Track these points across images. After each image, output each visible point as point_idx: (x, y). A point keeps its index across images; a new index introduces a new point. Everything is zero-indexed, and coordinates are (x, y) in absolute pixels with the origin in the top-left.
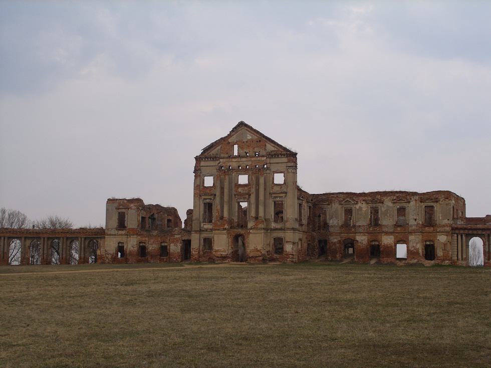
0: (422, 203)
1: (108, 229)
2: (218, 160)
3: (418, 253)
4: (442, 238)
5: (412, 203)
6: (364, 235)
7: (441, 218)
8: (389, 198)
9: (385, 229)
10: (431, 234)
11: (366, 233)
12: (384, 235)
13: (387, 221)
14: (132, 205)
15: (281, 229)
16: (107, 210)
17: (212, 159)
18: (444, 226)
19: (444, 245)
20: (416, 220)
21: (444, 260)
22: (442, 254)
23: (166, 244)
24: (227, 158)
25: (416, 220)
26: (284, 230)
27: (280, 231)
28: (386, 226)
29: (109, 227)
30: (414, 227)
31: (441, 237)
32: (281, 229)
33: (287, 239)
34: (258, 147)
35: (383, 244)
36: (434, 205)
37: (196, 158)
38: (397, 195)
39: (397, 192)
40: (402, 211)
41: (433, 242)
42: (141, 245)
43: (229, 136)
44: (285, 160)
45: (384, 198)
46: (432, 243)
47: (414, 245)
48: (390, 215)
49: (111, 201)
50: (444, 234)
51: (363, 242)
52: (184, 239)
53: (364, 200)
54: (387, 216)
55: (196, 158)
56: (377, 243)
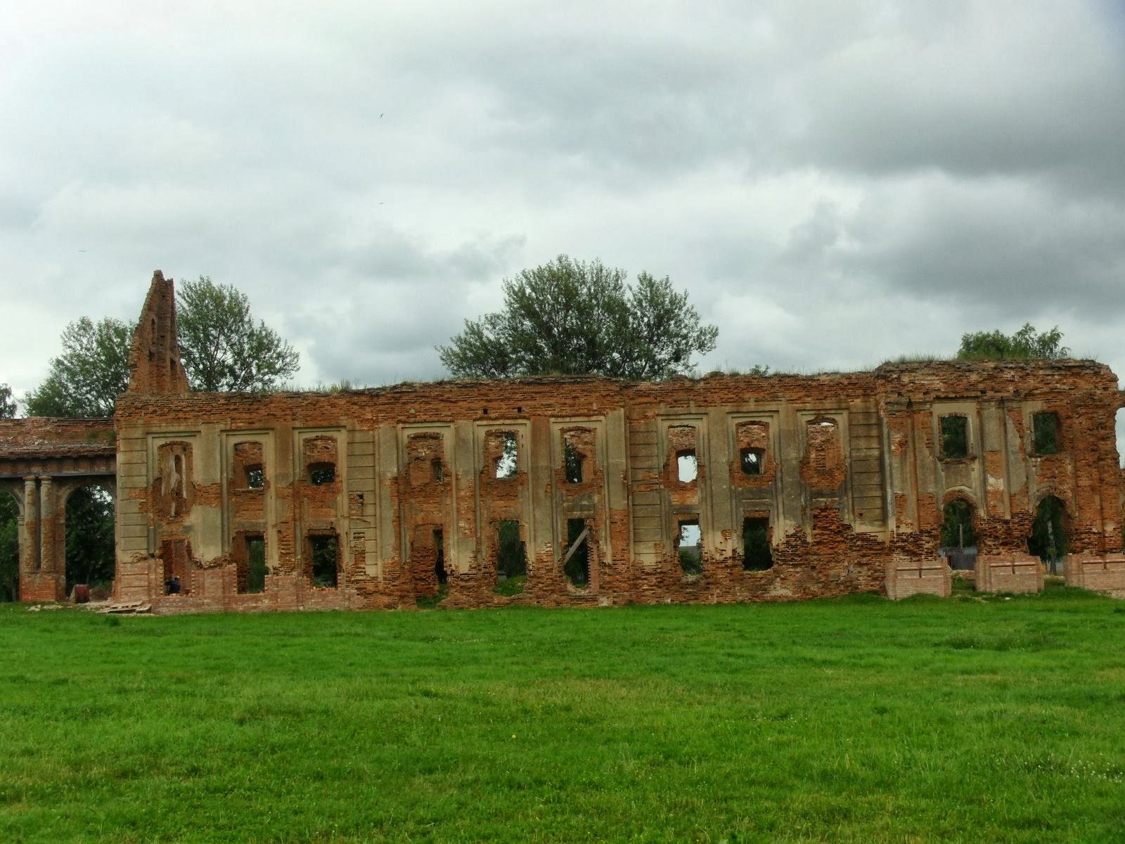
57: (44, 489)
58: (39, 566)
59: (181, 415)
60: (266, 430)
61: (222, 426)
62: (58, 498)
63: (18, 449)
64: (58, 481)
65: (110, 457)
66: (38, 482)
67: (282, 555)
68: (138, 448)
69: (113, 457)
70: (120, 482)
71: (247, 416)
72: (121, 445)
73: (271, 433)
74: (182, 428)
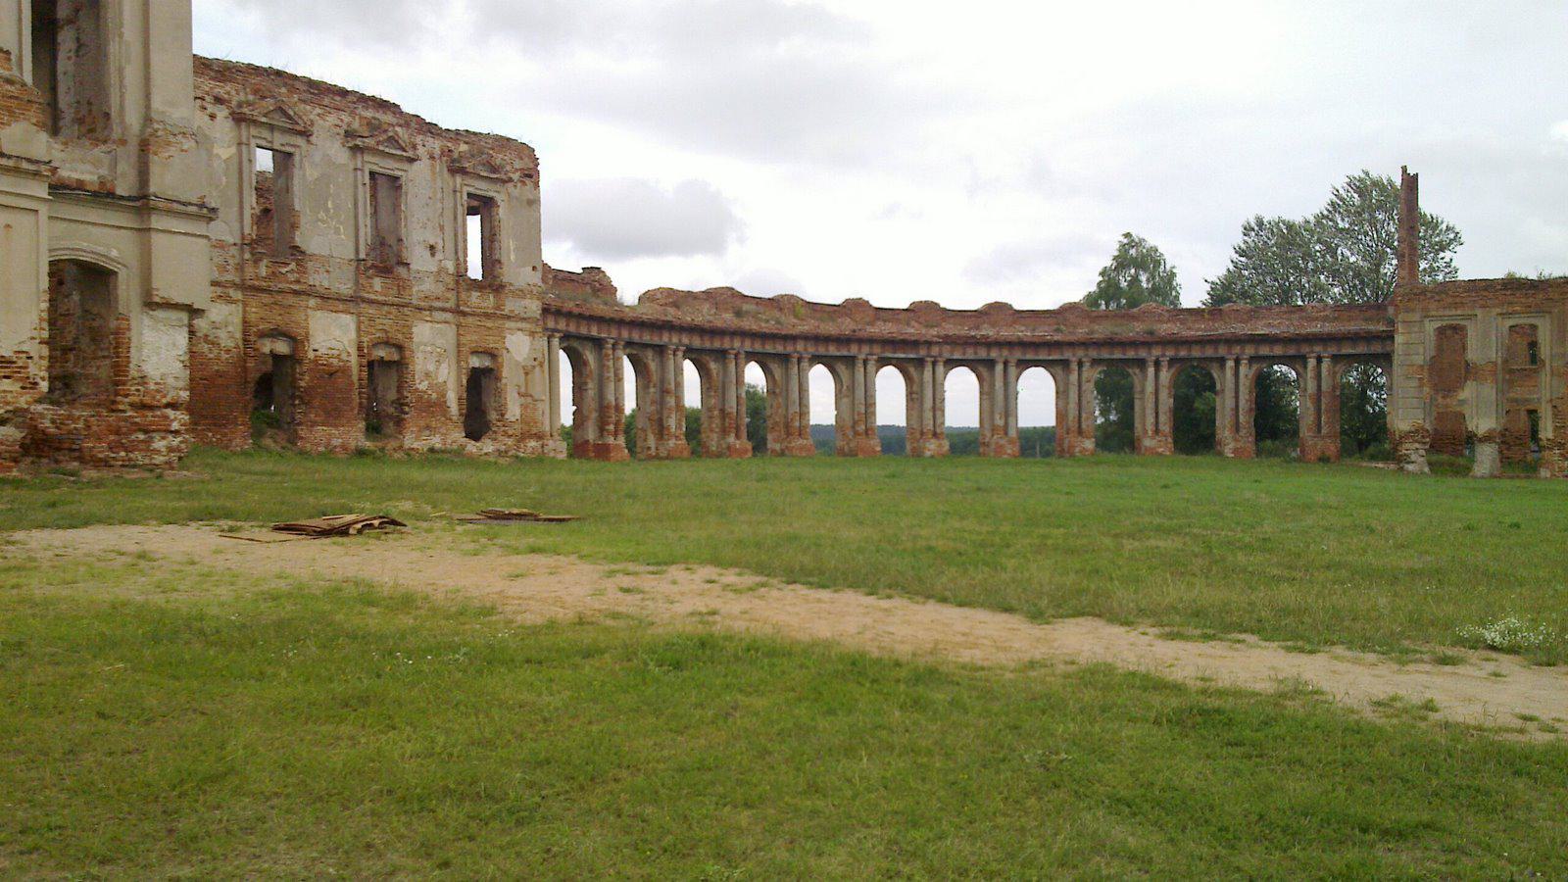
0: (459, 179)
3: (441, 405)
4: (519, 346)
5: (421, 168)
6: (230, 301)
7: (512, 257)
8: (332, 119)
9: (318, 279)
10: (489, 324)
11: (235, 285)
12: (318, 308)
13: (330, 236)
15: (103, 196)
18: (521, 294)
19: (527, 374)
20: (432, 248)
21: (523, 437)
22: (518, 412)
25: (432, 248)
26: (142, 203)
27: (94, 214)
28: (325, 261)
30: (428, 286)
31: (513, 338)
32: (103, 196)
33: (166, 286)
35: (311, 355)
36: (499, 198)
38: (369, 114)
39: (364, 99)
40: (386, 188)
41: (493, 355)
45: (310, 113)
46: (487, 363)
47: (431, 368)
48: (337, 207)
50: (524, 325)
51: (222, 334)
53: (218, 100)
54: (327, 210)
56: (282, 347)
57: (1325, 365)
58: (1319, 431)
59: (1458, 300)
60: (1540, 311)
61: (1498, 310)
62: (1335, 373)
63: (1303, 332)
64: (1336, 359)
65: (1390, 337)
66: (1319, 360)
67: (1556, 428)
68: (1416, 329)
69: (1392, 338)
70: (1397, 359)
71: (1523, 300)
72: (1400, 328)
73: (1547, 316)
74: (1459, 312)
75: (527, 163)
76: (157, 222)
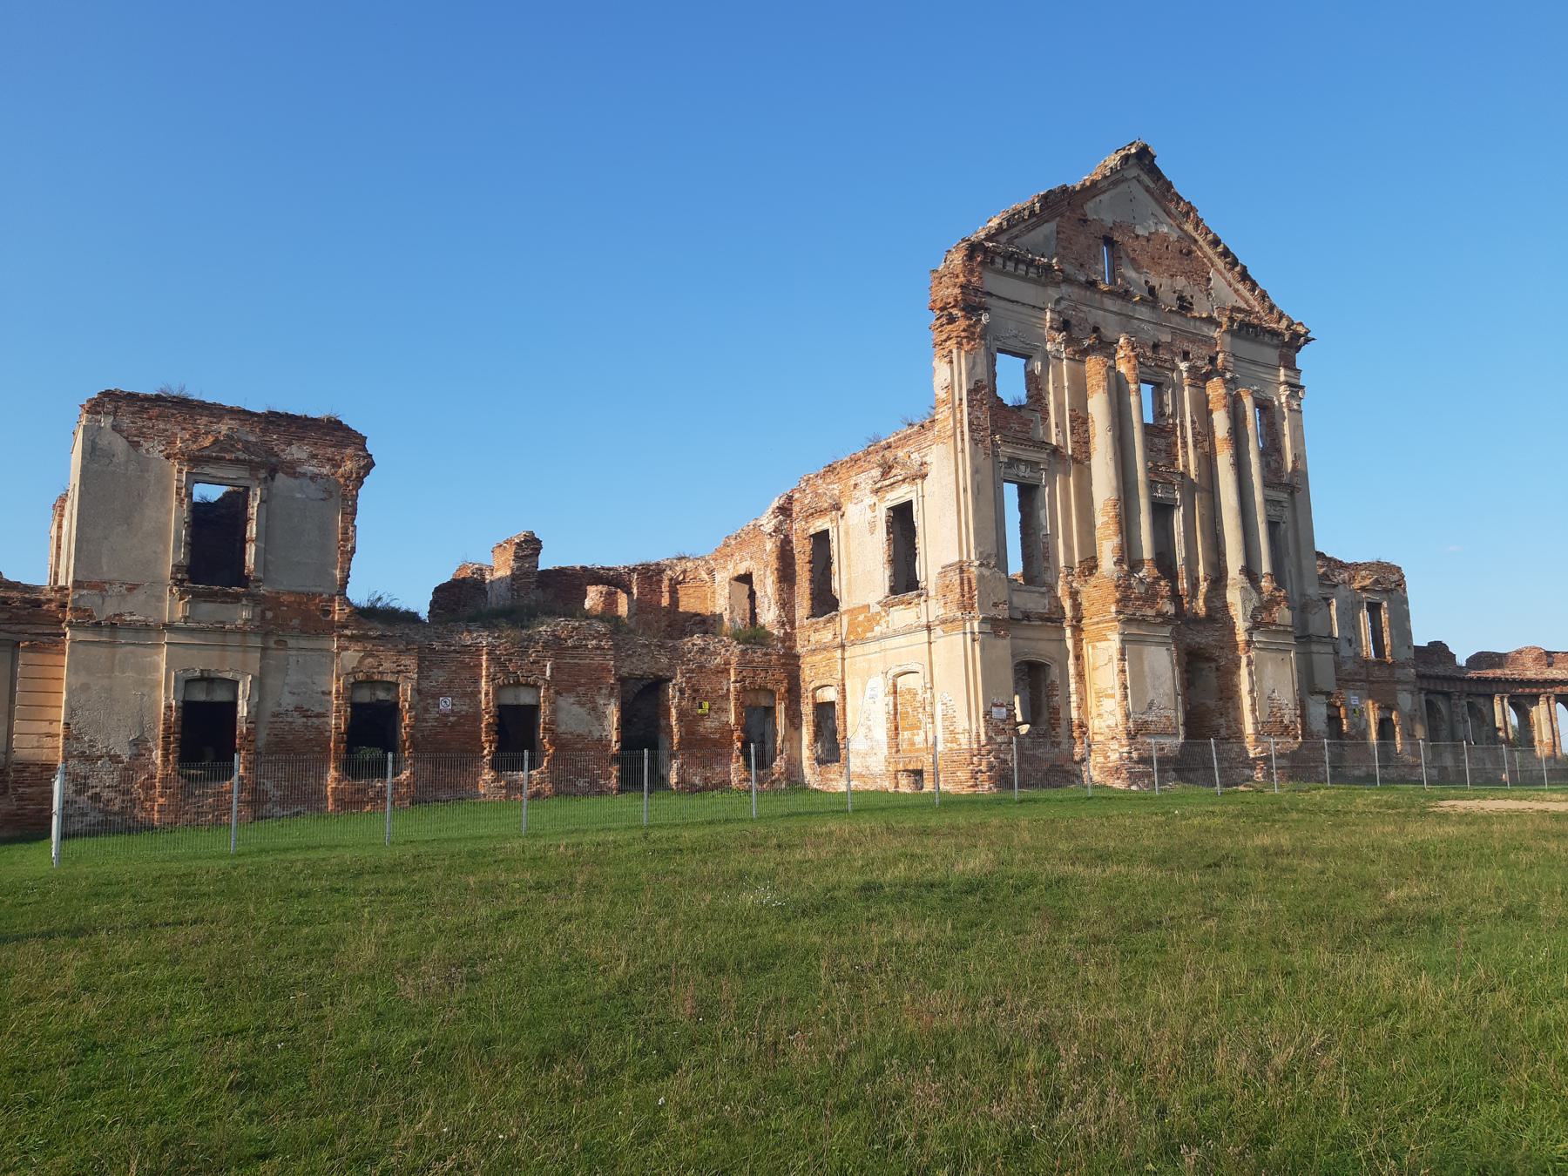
1: (100, 587)
2: (1057, 284)
14: (297, 452)
16: (92, 452)
17: (1032, 273)
23: (526, 698)
24: (1080, 285)
29: (106, 577)
34: (1184, 273)
37: (973, 249)
42: (364, 696)
43: (1091, 190)
44: (1272, 355)
49: (109, 402)
52: (624, 672)
55: (973, 249)
75: (1396, 577)
76: (1315, 648)
